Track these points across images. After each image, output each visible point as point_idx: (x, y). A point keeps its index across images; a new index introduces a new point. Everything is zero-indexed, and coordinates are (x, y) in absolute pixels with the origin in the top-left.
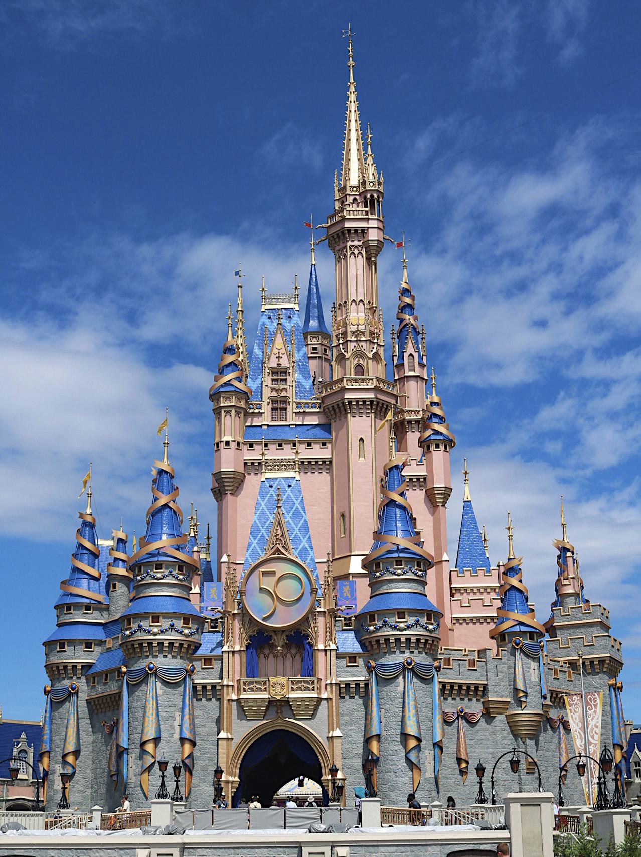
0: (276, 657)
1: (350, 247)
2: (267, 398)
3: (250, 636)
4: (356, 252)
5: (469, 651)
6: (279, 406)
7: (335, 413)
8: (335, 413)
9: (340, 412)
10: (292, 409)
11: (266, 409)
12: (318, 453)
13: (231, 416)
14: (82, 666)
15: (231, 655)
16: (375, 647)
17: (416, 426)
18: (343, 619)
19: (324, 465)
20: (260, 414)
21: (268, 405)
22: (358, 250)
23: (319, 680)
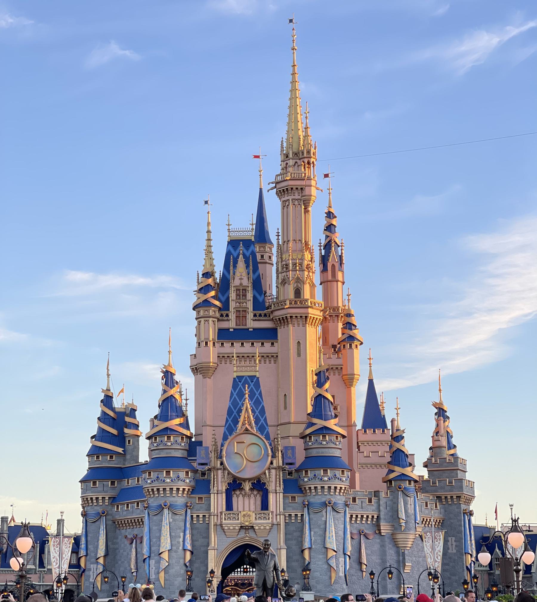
1: (292, 200)
2: (232, 309)
3: (228, 484)
7: (281, 323)
8: (281, 323)
9: (284, 322)
10: (250, 316)
11: (232, 316)
13: (208, 323)
14: (109, 497)
15: (216, 495)
16: (308, 491)
18: (287, 472)
19: (274, 357)
20: (228, 320)
21: (234, 314)
22: (298, 202)
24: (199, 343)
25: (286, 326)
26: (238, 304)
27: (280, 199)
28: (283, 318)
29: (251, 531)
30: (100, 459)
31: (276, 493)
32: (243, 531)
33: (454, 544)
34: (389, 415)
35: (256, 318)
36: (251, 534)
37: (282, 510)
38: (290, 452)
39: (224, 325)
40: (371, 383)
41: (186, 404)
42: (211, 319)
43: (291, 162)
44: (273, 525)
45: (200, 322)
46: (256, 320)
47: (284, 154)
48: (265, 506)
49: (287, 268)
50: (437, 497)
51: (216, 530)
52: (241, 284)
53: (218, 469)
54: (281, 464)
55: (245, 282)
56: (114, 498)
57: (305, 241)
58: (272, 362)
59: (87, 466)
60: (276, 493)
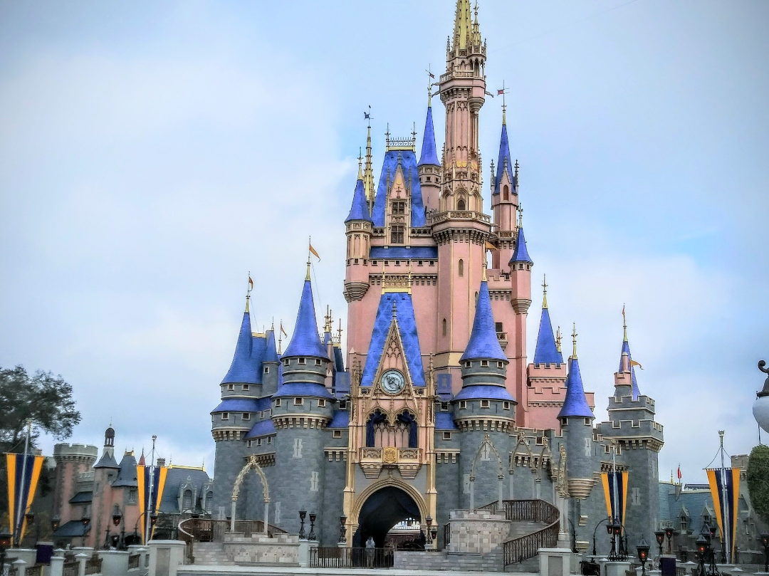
0: (389, 431)
3: (370, 415)
4: (462, 106)
5: (538, 430)
6: (397, 233)
9: (445, 238)
10: (407, 232)
11: (388, 233)
12: (426, 268)
17: (507, 245)
19: (433, 278)
20: (382, 237)
23: (421, 450)
24: (349, 261)
25: (447, 242)
26: (394, 219)
27: (445, 103)
28: (443, 233)
29: (394, 471)
30: (233, 389)
31: (426, 427)
32: (385, 472)
33: (639, 495)
34: (566, 350)
35: (415, 235)
36: (395, 474)
37: (432, 447)
38: (445, 380)
39: (378, 242)
40: (545, 311)
41: (340, 335)
42: (362, 234)
43: (458, 62)
44: (421, 465)
45: (350, 237)
46: (414, 237)
47: (450, 54)
48: (413, 442)
49: (450, 178)
50: (619, 441)
51: (353, 470)
52: (398, 197)
53: (358, 398)
54: (433, 393)
55: (403, 195)
56: (247, 432)
57: (471, 148)
58: (431, 283)
59: (220, 396)
60: (426, 427)
